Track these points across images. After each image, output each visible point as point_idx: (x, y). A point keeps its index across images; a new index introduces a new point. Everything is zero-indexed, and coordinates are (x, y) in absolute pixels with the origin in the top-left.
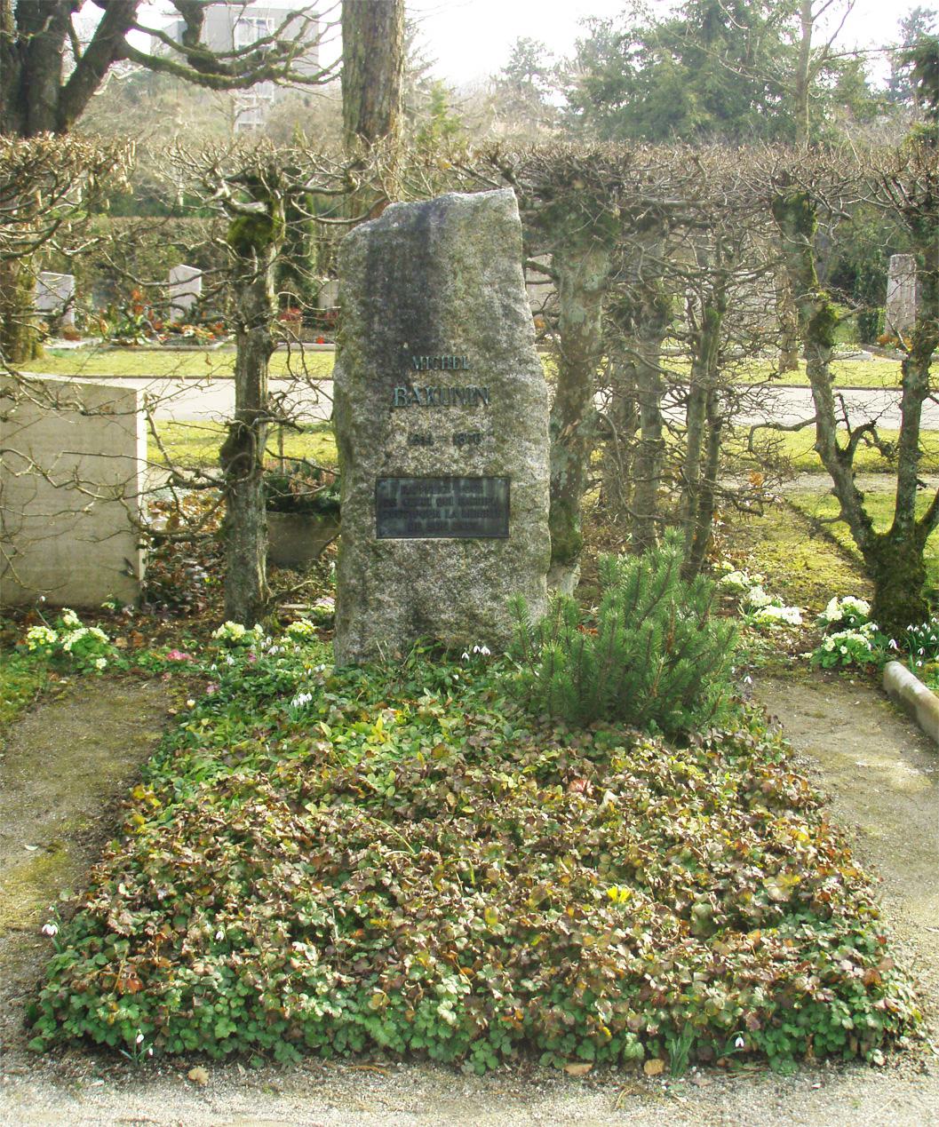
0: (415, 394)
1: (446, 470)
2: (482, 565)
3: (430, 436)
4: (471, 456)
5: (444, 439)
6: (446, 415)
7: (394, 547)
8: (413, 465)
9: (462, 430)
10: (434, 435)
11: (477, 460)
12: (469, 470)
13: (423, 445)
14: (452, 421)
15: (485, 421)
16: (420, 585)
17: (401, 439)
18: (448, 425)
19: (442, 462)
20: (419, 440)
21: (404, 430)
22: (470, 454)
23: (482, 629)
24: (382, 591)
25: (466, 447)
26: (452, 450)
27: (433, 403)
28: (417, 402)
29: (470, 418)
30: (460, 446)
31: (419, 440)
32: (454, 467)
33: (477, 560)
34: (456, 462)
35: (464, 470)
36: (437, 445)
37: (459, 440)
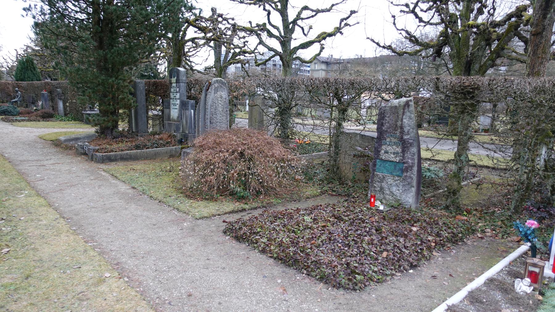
5: (391, 153)
16: (383, 184)
17: (383, 152)
20: (386, 152)
22: (396, 157)
26: (392, 156)
27: (389, 145)
31: (386, 152)
33: (395, 181)
37: (394, 153)
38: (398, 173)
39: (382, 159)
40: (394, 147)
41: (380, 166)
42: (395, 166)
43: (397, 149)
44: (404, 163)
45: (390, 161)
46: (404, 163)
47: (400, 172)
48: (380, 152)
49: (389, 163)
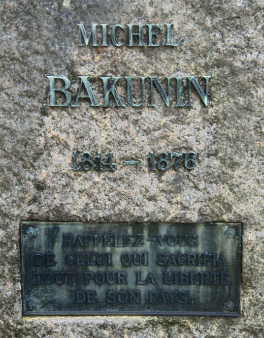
1: (137, 212)
3: (110, 158)
4: (179, 190)
5: (134, 162)
6: (136, 122)
8: (83, 200)
9: (163, 147)
10: (116, 155)
13: (98, 170)
14: (147, 132)
17: (62, 160)
19: (129, 199)
20: (93, 163)
21: (66, 146)
25: (170, 175)
26: (146, 180)
28: (87, 100)
29: (177, 128)
30: (161, 173)
32: (150, 207)
34: (152, 198)
36: (120, 172)
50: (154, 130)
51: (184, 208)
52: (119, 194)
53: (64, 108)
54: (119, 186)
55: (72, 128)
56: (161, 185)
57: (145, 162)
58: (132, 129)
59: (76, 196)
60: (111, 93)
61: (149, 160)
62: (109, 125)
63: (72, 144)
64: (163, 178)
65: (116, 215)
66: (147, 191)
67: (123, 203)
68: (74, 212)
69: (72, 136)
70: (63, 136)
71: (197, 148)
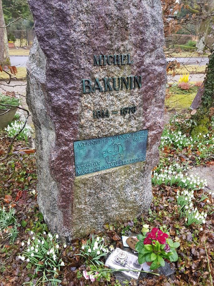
0: (97, 84)
1: (117, 132)
2: (131, 176)
3: (107, 112)
4: (130, 121)
5: (114, 112)
6: (116, 97)
7: (88, 180)
8: (97, 131)
9: (126, 106)
10: (110, 110)
11: (133, 122)
12: (129, 129)
13: (103, 117)
15: (138, 99)
16: (102, 195)
17: (88, 115)
18: (118, 103)
20: (101, 114)
22: (129, 120)
23: (130, 205)
24: (80, 203)
25: (127, 116)
26: (120, 119)
29: (130, 97)
30: (125, 115)
31: (101, 114)
32: (121, 129)
34: (122, 126)
35: (125, 129)
36: (111, 116)
37: (123, 112)
38: (135, 157)
39: (89, 138)
40: (123, 93)
41: (87, 156)
42: (128, 143)
43: (131, 99)
44: (150, 129)
45: (117, 135)
46: (150, 129)
47: (139, 152)
48: (78, 117)
49: (110, 141)
50: (123, 99)
51: (132, 127)
52: (111, 125)
53: (89, 93)
54: (111, 122)
55: (93, 101)
56: (125, 120)
57: (119, 112)
58: (115, 99)
59: (95, 129)
60: (108, 85)
61: (121, 111)
62: (107, 98)
63: (92, 108)
64: (125, 117)
65: (110, 133)
66: (120, 123)
67: (112, 129)
68: (94, 135)
69: (92, 104)
70: (89, 105)
71: (137, 104)
